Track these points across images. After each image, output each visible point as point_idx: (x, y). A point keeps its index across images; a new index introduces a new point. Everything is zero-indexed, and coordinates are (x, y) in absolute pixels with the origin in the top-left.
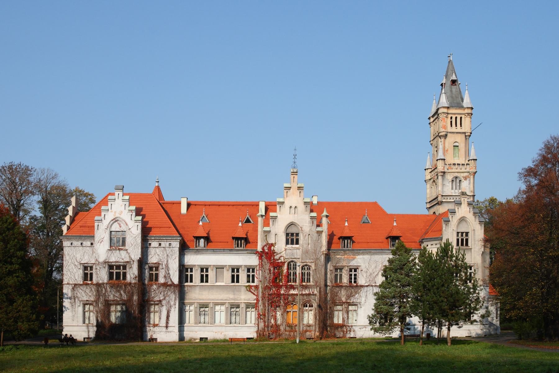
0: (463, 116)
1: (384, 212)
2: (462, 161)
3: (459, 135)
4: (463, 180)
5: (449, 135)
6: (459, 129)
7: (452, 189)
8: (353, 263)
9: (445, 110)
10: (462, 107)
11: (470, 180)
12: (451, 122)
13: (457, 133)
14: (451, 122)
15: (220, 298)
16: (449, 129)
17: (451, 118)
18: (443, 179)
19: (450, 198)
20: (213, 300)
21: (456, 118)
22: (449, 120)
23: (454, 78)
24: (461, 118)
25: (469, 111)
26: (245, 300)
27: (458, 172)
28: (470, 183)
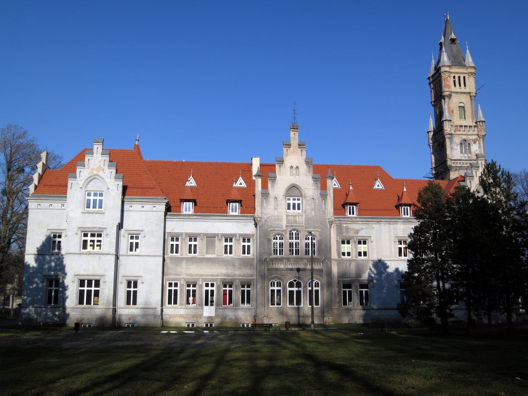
0: (466, 76)
1: (391, 178)
2: (469, 122)
3: (464, 95)
4: (472, 143)
5: (453, 95)
6: (463, 89)
7: (461, 152)
8: (362, 234)
9: (447, 69)
10: (463, 66)
11: (479, 144)
12: (454, 81)
13: (462, 93)
14: (454, 81)
15: (210, 274)
16: (453, 89)
17: (454, 77)
18: (451, 143)
19: (463, 163)
20: (202, 275)
21: (459, 77)
22: (452, 80)
23: (453, 36)
24: (464, 77)
25: (473, 70)
26: (239, 276)
27: (466, 135)
28: (480, 147)
